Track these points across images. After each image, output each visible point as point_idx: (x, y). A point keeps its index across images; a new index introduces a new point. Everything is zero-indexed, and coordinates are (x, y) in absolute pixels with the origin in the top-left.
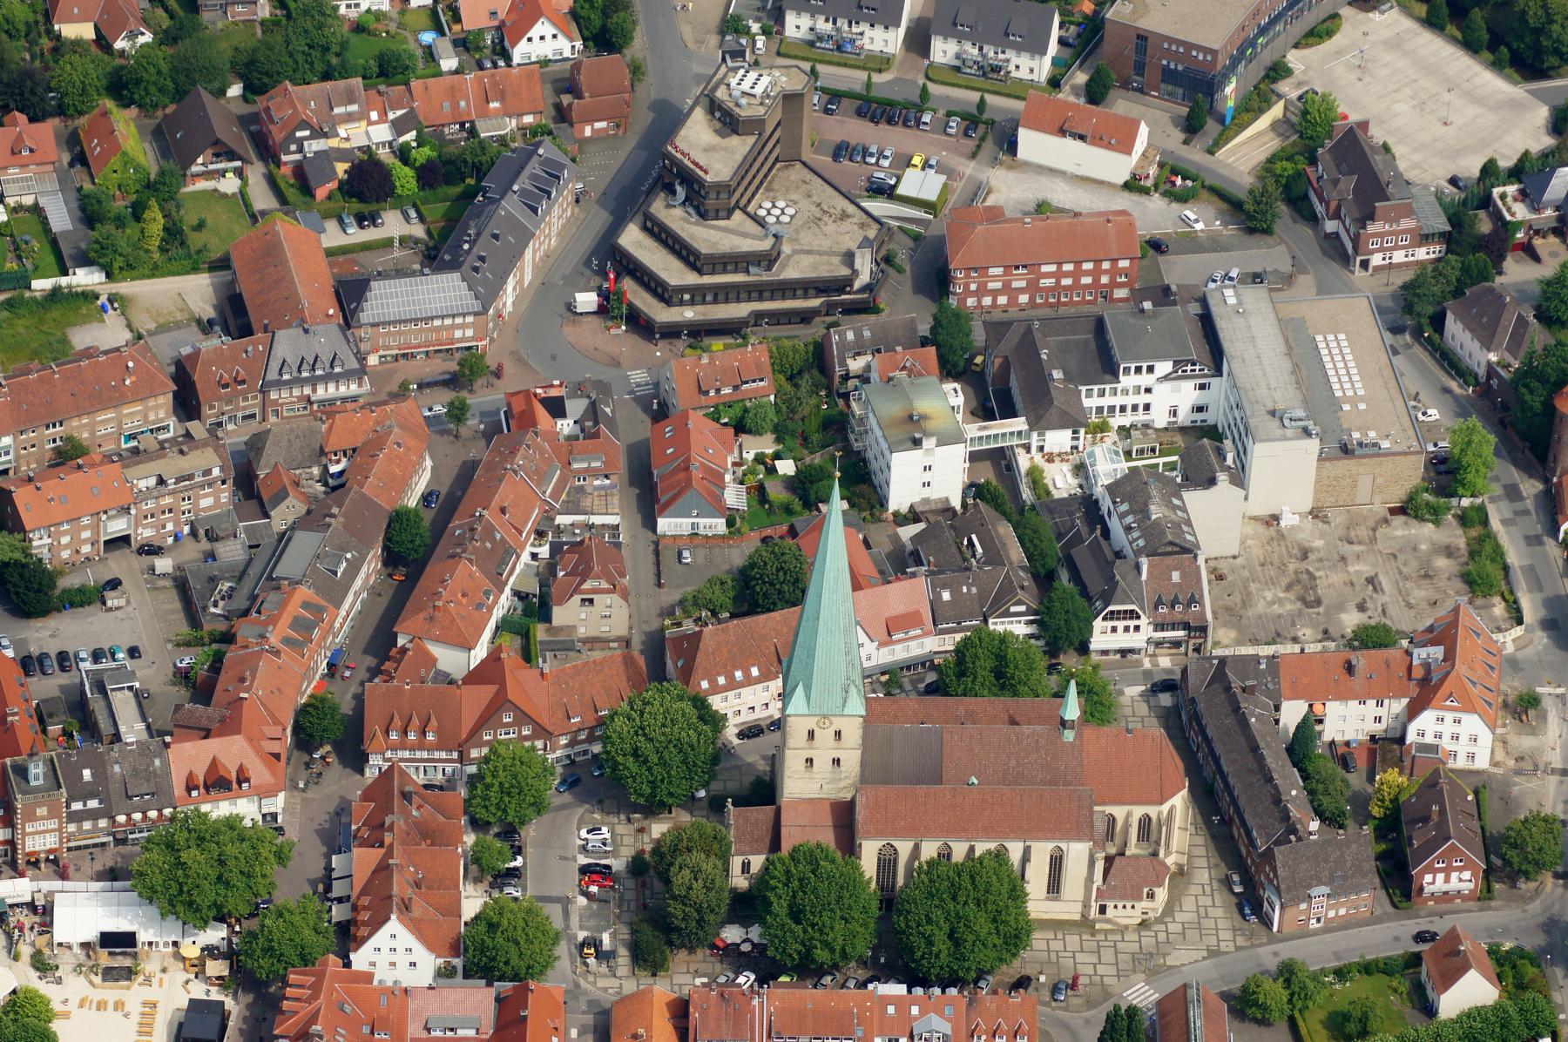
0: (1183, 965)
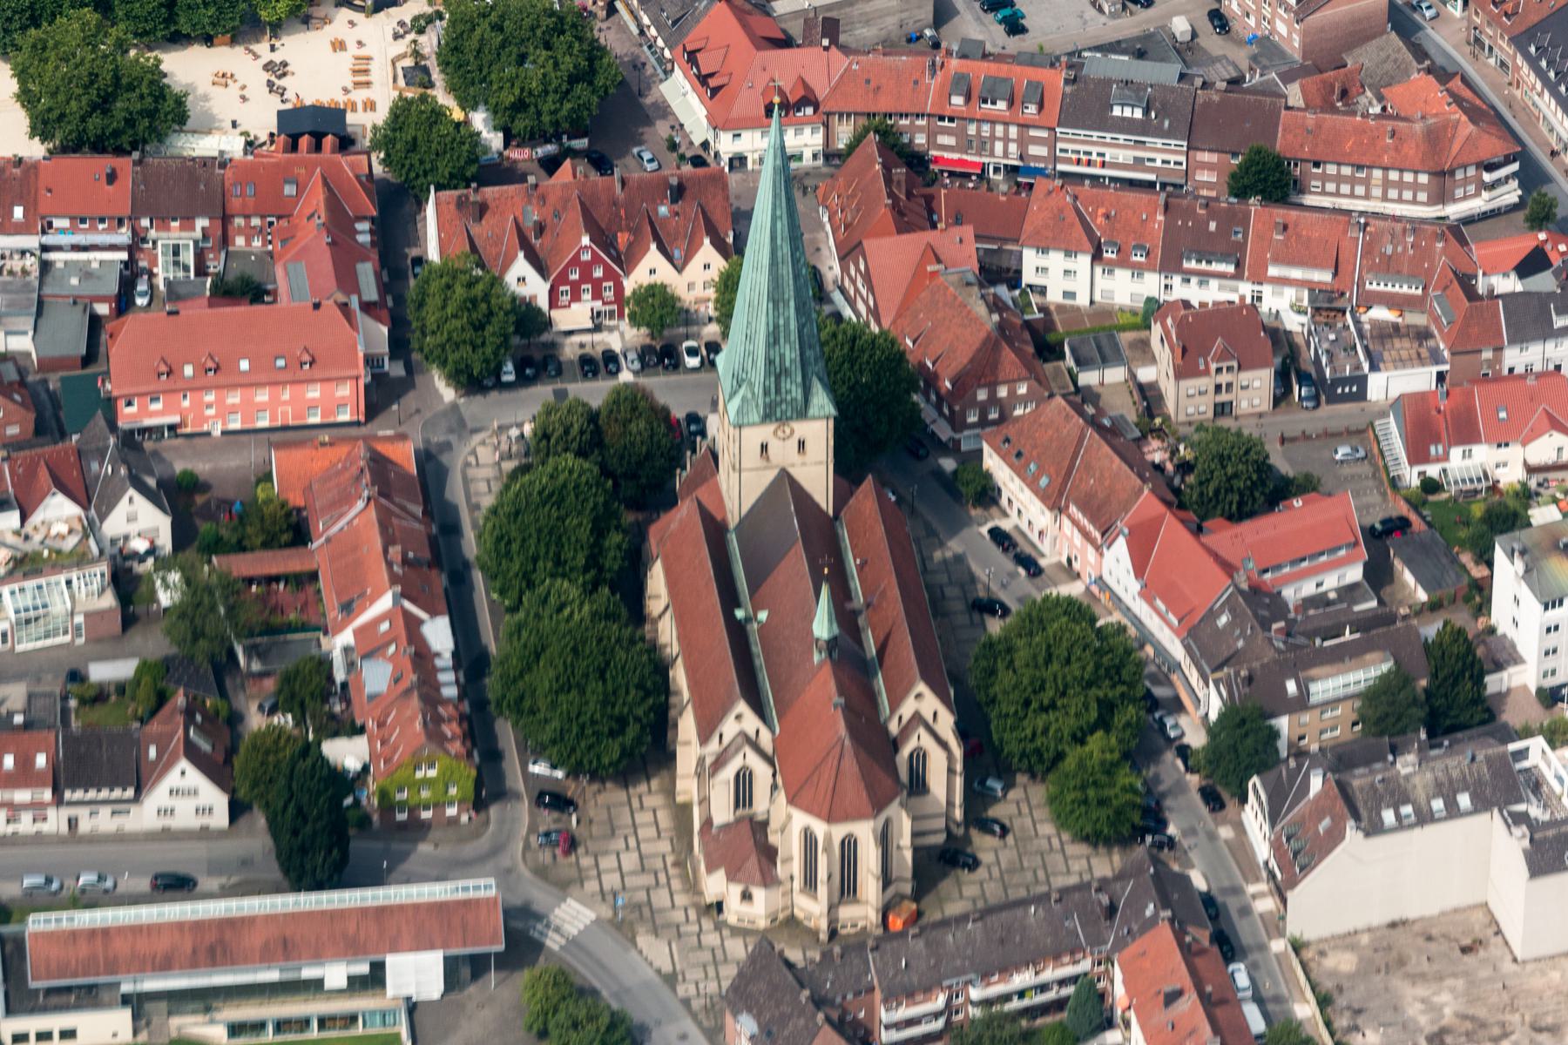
0: (641, 952)
